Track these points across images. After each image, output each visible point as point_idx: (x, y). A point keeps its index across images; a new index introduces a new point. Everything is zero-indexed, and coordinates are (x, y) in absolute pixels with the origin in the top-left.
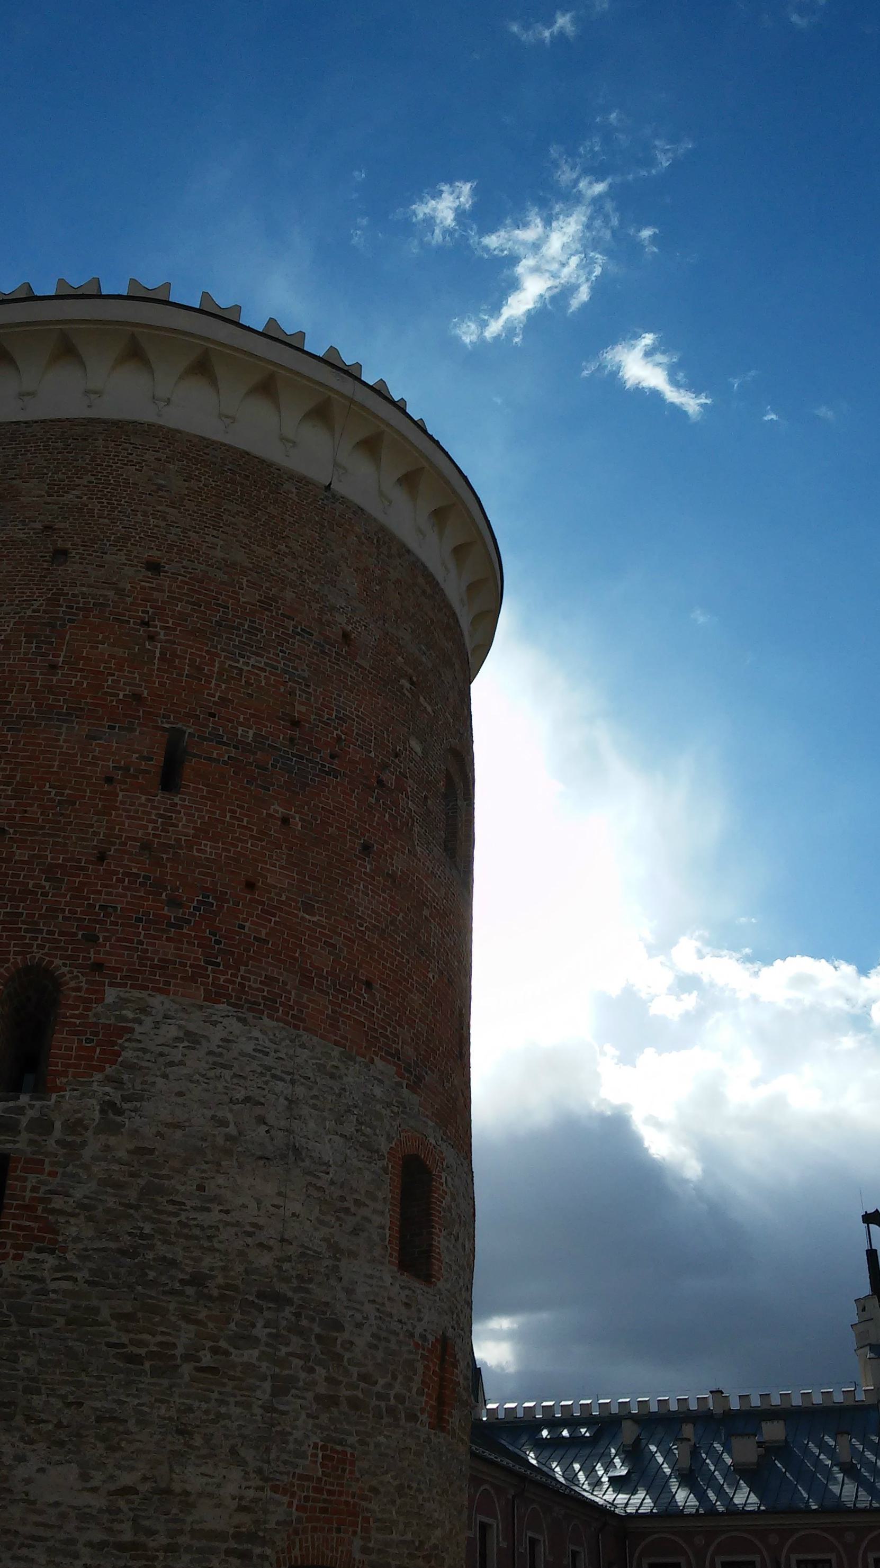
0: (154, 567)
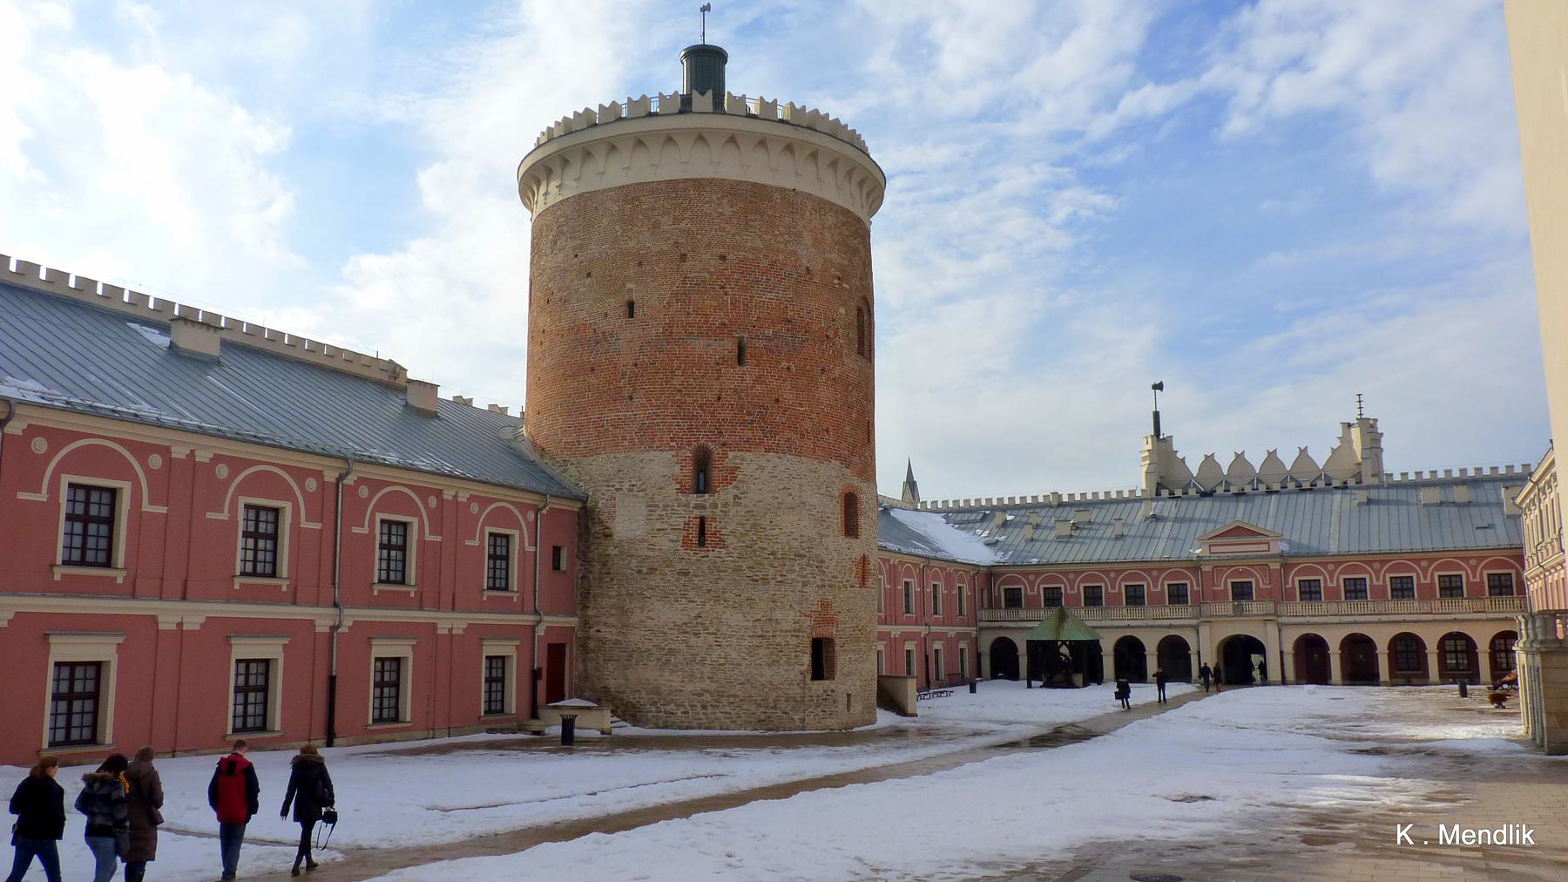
0: (723, 258)
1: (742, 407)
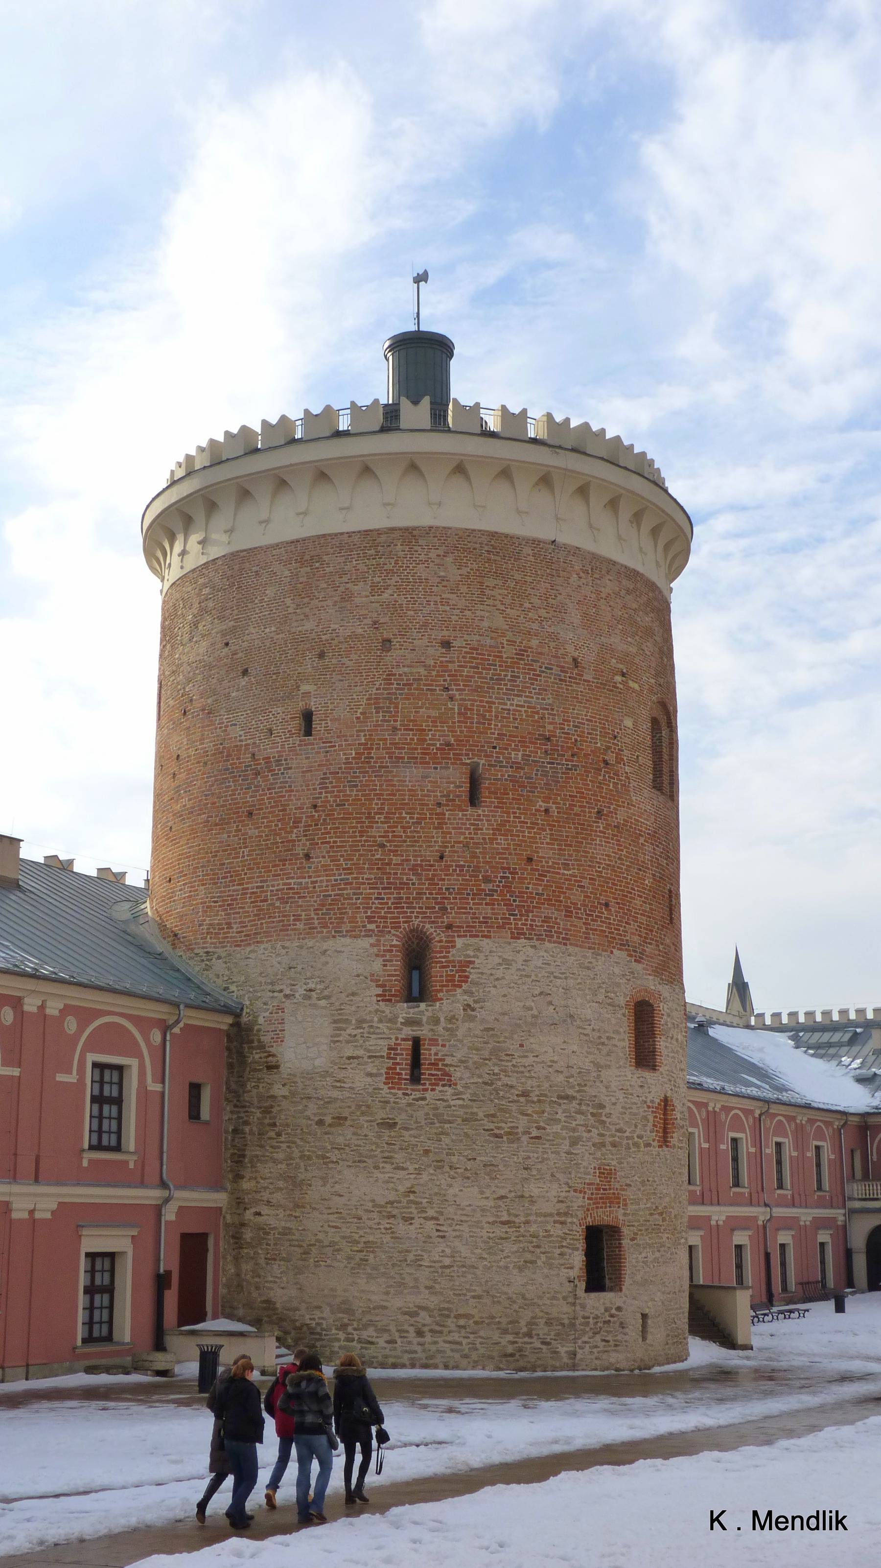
1: (477, 869)
